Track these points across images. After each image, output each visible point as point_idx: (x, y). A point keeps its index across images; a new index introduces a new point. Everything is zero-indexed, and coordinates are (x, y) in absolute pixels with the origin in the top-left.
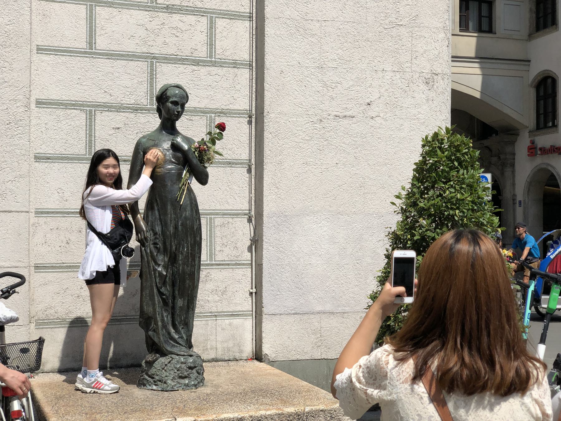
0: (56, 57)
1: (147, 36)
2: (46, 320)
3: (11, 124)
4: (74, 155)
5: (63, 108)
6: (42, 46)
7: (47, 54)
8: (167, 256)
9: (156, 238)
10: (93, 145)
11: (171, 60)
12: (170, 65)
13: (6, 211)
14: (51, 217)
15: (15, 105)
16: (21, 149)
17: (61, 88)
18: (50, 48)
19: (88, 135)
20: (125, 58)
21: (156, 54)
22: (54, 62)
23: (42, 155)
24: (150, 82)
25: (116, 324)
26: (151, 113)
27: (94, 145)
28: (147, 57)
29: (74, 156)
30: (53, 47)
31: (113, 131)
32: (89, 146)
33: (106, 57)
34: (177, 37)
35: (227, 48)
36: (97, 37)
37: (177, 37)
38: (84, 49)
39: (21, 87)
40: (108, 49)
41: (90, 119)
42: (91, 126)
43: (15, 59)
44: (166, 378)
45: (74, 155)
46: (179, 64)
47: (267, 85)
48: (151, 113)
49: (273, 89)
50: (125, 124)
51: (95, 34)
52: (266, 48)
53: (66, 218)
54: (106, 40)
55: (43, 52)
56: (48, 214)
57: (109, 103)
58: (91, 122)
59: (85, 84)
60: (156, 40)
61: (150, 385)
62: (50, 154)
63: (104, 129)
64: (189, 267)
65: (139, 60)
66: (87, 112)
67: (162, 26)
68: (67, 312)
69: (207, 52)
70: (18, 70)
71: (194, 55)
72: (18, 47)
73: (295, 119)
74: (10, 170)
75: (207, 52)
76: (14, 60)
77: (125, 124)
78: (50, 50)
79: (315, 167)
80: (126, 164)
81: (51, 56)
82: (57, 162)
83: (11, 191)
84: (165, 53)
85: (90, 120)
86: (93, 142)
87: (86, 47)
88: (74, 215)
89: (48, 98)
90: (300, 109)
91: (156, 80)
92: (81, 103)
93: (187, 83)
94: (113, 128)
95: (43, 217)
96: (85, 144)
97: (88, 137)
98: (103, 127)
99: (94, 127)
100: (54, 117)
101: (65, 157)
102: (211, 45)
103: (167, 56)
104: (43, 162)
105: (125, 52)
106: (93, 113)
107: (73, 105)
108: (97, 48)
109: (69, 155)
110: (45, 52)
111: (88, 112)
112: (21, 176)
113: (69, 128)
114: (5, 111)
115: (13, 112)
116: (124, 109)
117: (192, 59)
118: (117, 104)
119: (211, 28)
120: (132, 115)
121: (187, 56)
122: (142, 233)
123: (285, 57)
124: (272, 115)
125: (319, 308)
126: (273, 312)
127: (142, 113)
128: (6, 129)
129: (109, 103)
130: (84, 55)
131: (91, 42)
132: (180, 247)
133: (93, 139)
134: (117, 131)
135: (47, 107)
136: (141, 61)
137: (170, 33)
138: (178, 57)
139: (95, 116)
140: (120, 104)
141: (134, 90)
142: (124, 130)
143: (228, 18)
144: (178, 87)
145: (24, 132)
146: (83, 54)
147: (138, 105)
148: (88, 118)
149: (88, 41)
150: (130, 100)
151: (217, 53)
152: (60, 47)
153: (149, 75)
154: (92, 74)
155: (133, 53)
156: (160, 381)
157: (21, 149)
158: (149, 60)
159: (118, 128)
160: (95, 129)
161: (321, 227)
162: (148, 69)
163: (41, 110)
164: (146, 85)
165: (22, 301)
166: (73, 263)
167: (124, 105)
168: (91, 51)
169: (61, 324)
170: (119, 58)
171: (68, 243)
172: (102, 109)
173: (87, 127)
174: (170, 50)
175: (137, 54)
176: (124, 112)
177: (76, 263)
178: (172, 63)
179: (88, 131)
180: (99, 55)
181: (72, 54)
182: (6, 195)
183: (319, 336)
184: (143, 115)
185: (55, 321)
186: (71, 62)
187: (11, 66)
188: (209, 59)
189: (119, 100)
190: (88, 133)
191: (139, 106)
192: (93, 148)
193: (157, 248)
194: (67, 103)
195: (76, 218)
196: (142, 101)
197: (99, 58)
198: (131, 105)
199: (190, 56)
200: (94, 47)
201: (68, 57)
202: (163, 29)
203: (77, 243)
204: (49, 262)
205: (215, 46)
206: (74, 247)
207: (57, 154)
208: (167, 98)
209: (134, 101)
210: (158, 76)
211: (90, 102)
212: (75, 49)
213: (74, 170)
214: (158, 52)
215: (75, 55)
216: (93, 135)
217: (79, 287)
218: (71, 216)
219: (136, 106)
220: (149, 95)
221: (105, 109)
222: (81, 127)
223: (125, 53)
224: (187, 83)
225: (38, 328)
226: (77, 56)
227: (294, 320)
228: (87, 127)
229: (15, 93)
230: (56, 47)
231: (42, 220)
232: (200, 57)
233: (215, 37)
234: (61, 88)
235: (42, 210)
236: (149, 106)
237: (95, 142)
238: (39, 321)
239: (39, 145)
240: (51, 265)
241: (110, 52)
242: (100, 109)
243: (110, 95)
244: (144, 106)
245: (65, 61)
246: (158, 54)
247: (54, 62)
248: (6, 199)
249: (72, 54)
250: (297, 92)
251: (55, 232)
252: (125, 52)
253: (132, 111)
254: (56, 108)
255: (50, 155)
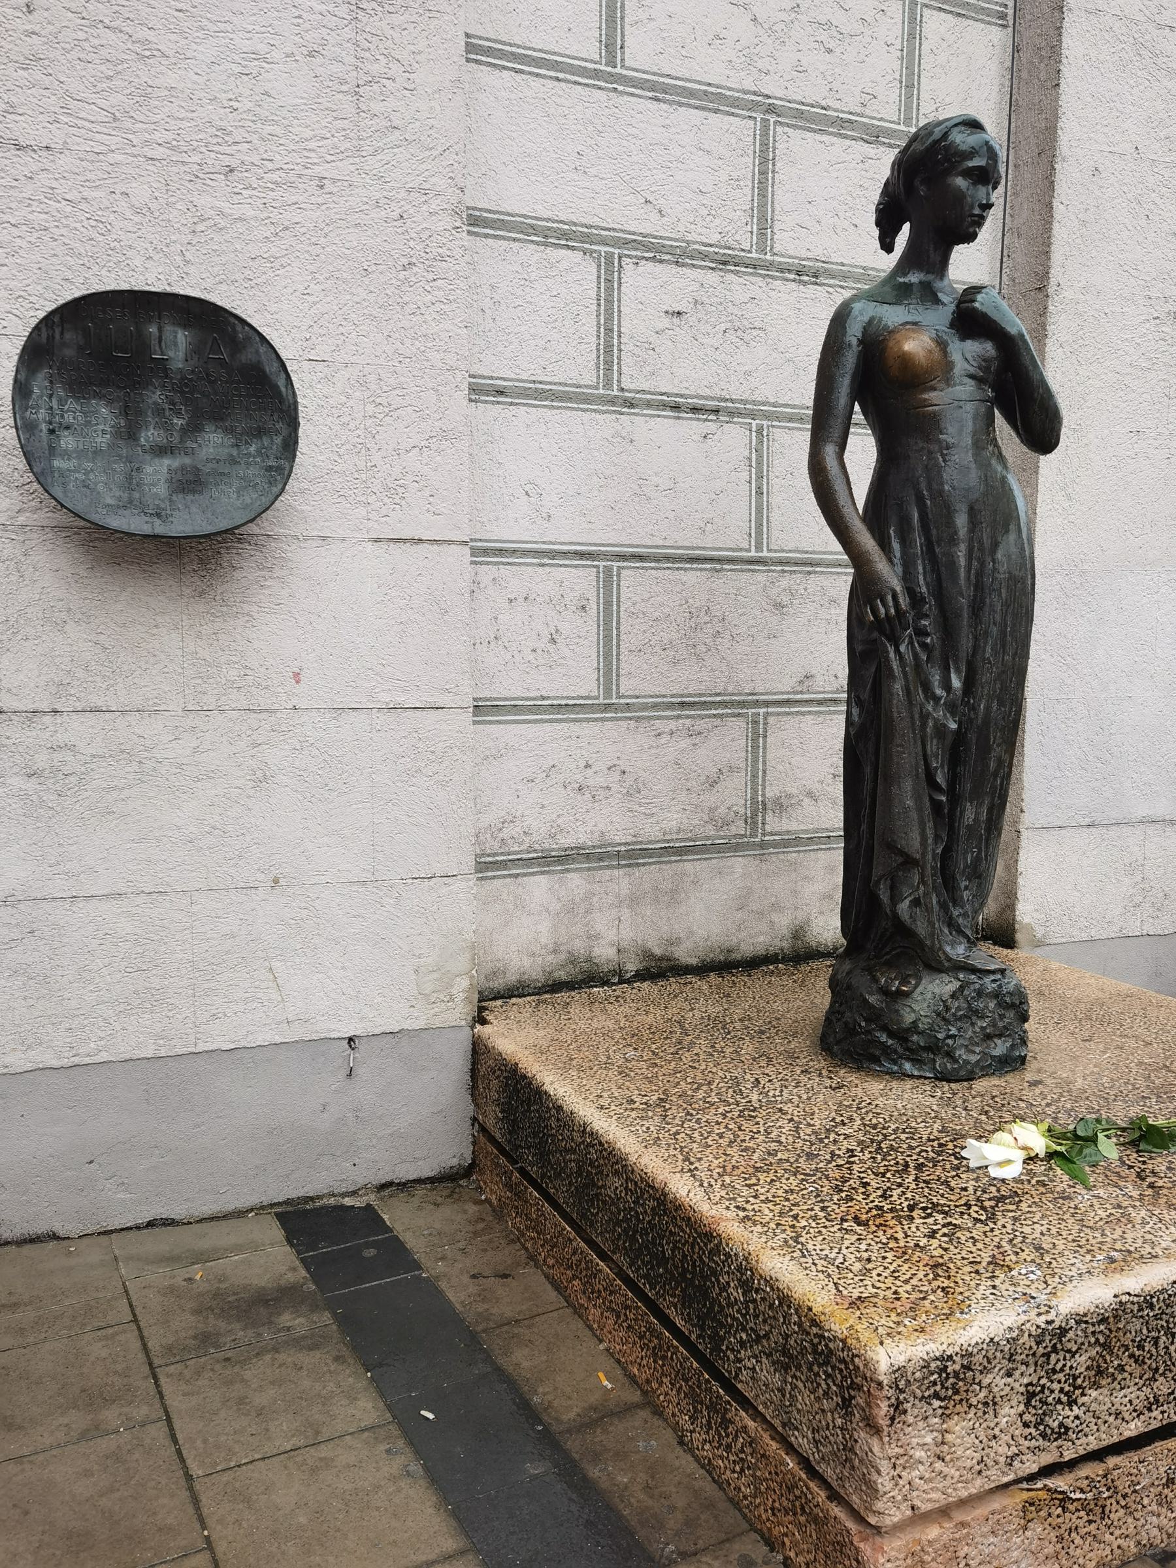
0: (519, 77)
1: (756, 41)
2: (502, 854)
3: (415, 269)
4: (566, 385)
5: (537, 243)
6: (481, 38)
7: (494, 65)
8: (958, 671)
9: (921, 615)
10: (616, 361)
11: (813, 122)
12: (809, 134)
13: (404, 541)
14: (508, 564)
15: (425, 208)
16: (445, 351)
17: (533, 179)
18: (500, 47)
19: (602, 330)
20: (698, 103)
21: (776, 98)
22: (513, 96)
23: (483, 381)
24: (760, 182)
25: (670, 862)
26: (761, 275)
27: (619, 358)
28: (753, 106)
29: (567, 389)
30: (510, 45)
31: (665, 322)
32: (606, 363)
33: (650, 94)
34: (829, 51)
35: (948, 100)
36: (627, 27)
37: (829, 51)
38: (592, 61)
39: (441, 149)
40: (655, 69)
41: (609, 281)
42: (609, 301)
43: (420, 53)
44: (950, 1042)
45: (566, 385)
46: (831, 134)
47: (1061, 206)
48: (761, 275)
49: (1073, 218)
50: (696, 302)
51: (622, 18)
52: (1063, 96)
53: (547, 569)
54: (651, 39)
55: (483, 58)
56: (502, 556)
57: (655, 237)
58: (610, 289)
59: (593, 171)
60: (777, 54)
61: (895, 1063)
62: (504, 379)
63: (643, 314)
64: (1004, 706)
65: (733, 110)
66: (599, 259)
67: (793, 15)
68: (553, 831)
69: (900, 105)
70: (430, 91)
71: (868, 112)
72: (428, 14)
73: (1118, 310)
74: (414, 415)
75: (900, 105)
76: (418, 58)
77: (696, 302)
78: (502, 54)
79: (1155, 443)
80: (698, 419)
81: (505, 73)
82: (525, 405)
83: (417, 479)
84: (799, 98)
85: (609, 284)
86: (615, 351)
87: (597, 57)
88: (567, 562)
89: (495, 208)
90: (1132, 280)
91: (773, 178)
92: (586, 230)
93: (850, 193)
94: (666, 312)
95: (488, 563)
96: (594, 356)
97: (602, 335)
98: (640, 306)
99: (619, 306)
100: (515, 268)
101: (544, 391)
102: (910, 86)
103: (803, 108)
104: (486, 402)
105: (699, 82)
106: (616, 265)
107: (564, 235)
108: (627, 64)
109: (555, 384)
110: (489, 60)
111: (603, 260)
112: (445, 434)
113: (553, 304)
114: (395, 223)
115: (419, 228)
116: (692, 258)
117: (864, 124)
118: (676, 240)
119: (911, 36)
120: (713, 278)
121: (851, 113)
122: (889, 598)
123: (1106, 130)
124: (1068, 294)
125: (1141, 811)
126: (1043, 822)
127: (737, 273)
128: (399, 283)
129: (655, 237)
130: (592, 82)
131: (612, 46)
132: (986, 643)
133: (616, 341)
134: (675, 320)
135: (495, 237)
136: (737, 115)
137: (812, 39)
138: (828, 113)
139: (620, 273)
140: (683, 241)
141: (720, 201)
142: (693, 320)
143: (951, 12)
144: (974, 125)
145: (452, 298)
146: (591, 78)
147: (729, 248)
148: (603, 276)
149: (604, 37)
150: (707, 233)
151: (921, 112)
152: (529, 49)
153: (757, 162)
154: (613, 142)
155: (719, 90)
156: (928, 1049)
157: (445, 351)
158: (759, 116)
159: (678, 313)
160: (620, 311)
161: (1158, 601)
162: (754, 143)
163: (481, 242)
164: (748, 191)
165: (455, 807)
166: (568, 698)
167: (696, 247)
168: (613, 70)
169: (539, 865)
170: (683, 100)
171: (553, 641)
172: (639, 253)
173: (599, 305)
174: (809, 91)
175: (728, 93)
176: (693, 265)
177: (573, 698)
178: (815, 131)
179: (602, 317)
180: (633, 86)
181: (561, 75)
182: (400, 490)
183: (1138, 878)
184: (741, 280)
185: (524, 856)
186: (558, 101)
187: (412, 76)
188: (902, 127)
189: (682, 229)
190: (602, 322)
191: (730, 252)
192: (615, 368)
193: (924, 645)
194: (549, 229)
195: (572, 570)
196: (737, 237)
197: (632, 95)
198: (711, 246)
199: (858, 115)
200: (619, 58)
201: (550, 84)
202: (796, 23)
203: (577, 640)
204: (505, 694)
205: (918, 89)
206: (568, 653)
207: (523, 381)
208: (949, 161)
209: (719, 236)
210: (778, 165)
211: (609, 229)
212: (569, 61)
213: (566, 430)
214: (780, 94)
215: (569, 77)
216: (616, 329)
217: (582, 764)
218: (561, 562)
219: (722, 251)
220: (755, 220)
221: (646, 255)
222: (585, 302)
223: (698, 87)
224: (850, 193)
225: (486, 878)
226: (575, 83)
227: (1087, 841)
228: (599, 305)
229: (424, 166)
230: (519, 47)
231: (487, 573)
232: (881, 119)
233: (919, 66)
234: (533, 179)
235: (485, 544)
236: (754, 255)
237: (620, 350)
238: (483, 860)
239: (476, 349)
240: (512, 703)
241: (662, 80)
242: (634, 253)
243: (660, 212)
244: (743, 254)
245: (541, 95)
246: (781, 99)
247: (513, 96)
248: (403, 503)
249: (561, 75)
250: (1127, 233)
251: (519, 609)
252: (699, 82)
253: (714, 265)
254: (519, 240)
255: (505, 383)
